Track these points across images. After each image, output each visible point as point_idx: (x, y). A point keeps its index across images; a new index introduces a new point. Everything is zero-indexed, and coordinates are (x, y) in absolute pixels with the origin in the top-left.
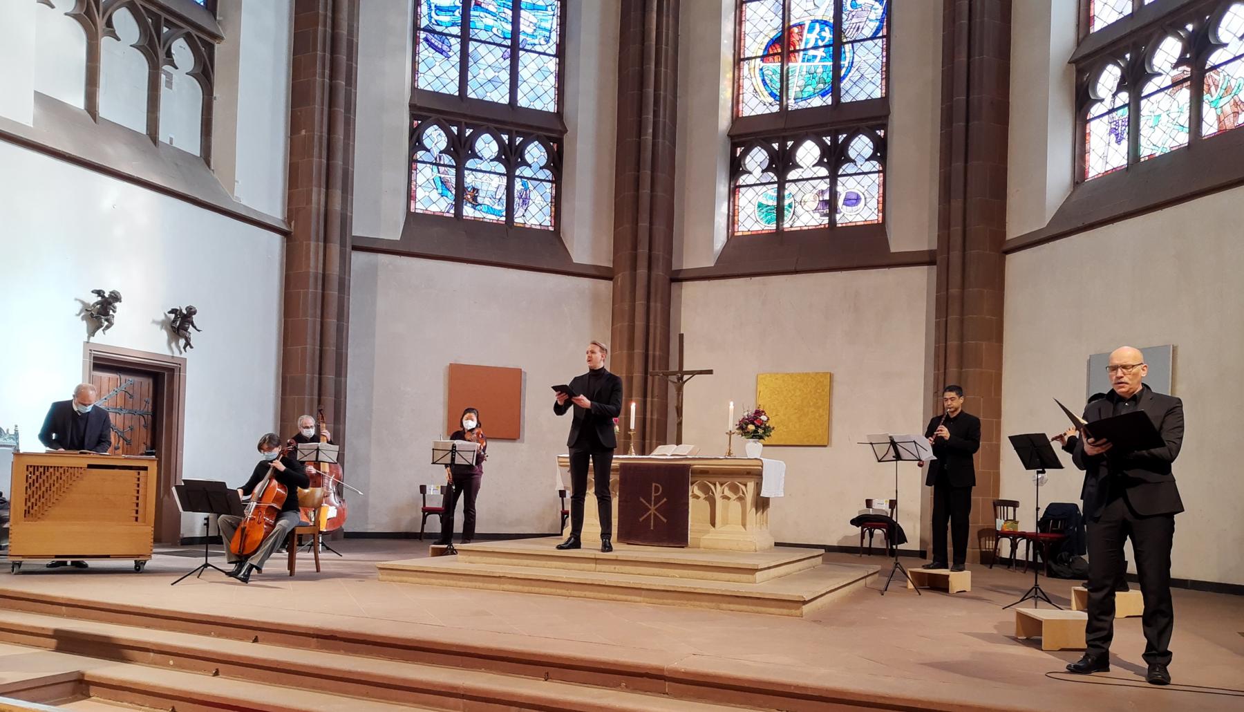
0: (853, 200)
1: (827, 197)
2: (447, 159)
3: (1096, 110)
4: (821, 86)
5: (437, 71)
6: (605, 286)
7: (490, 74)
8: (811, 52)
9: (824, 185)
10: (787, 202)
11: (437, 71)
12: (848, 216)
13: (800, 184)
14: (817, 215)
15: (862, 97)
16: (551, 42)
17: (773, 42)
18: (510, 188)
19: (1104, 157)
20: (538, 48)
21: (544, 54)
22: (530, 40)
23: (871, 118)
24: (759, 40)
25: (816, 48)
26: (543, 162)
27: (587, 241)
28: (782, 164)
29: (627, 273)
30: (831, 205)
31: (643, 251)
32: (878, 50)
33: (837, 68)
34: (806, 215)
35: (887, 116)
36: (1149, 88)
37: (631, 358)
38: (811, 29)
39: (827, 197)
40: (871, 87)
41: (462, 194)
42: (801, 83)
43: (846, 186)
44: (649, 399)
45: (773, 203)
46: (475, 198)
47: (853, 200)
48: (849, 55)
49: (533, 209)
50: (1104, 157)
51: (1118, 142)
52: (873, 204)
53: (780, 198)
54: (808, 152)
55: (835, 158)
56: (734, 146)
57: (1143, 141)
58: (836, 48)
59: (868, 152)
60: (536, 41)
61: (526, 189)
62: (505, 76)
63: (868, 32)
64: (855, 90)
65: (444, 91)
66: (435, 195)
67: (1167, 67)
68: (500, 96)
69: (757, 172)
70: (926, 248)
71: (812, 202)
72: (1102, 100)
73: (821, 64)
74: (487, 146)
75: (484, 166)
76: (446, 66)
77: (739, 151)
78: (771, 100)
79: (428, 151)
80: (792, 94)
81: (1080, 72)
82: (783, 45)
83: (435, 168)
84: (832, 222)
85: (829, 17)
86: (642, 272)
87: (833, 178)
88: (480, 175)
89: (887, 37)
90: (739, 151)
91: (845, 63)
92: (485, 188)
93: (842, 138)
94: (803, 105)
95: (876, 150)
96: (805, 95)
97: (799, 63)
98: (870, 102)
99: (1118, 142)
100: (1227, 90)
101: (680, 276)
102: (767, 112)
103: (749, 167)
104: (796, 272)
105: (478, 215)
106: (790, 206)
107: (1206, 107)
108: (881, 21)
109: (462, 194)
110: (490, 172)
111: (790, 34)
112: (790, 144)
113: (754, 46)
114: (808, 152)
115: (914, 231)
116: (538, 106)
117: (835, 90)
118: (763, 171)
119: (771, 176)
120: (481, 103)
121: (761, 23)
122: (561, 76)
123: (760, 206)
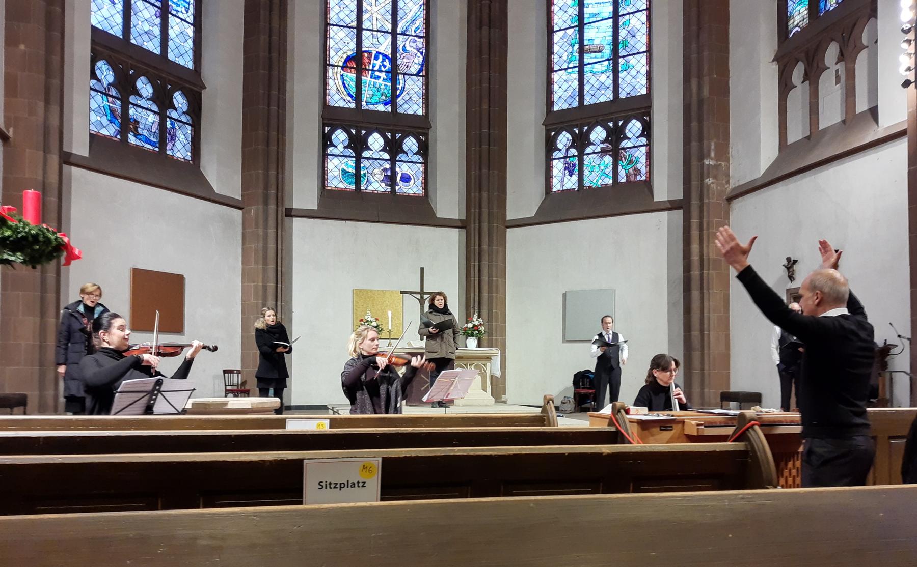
0: (406, 179)
1: (389, 173)
2: (113, 92)
3: (556, 154)
4: (384, 98)
6: (237, 214)
7: (147, 27)
8: (377, 73)
9: (388, 166)
10: (362, 172)
12: (403, 188)
13: (371, 161)
14: (383, 185)
15: (411, 112)
16: (190, 14)
17: (348, 59)
18: (162, 125)
19: (562, 181)
20: (180, 15)
24: (340, 53)
25: (380, 71)
26: (185, 109)
28: (358, 145)
29: (261, 207)
30: (391, 179)
31: (272, 192)
32: (420, 84)
33: (394, 88)
34: (376, 185)
36: (589, 150)
37: (265, 271)
38: (376, 58)
39: (389, 173)
40: (415, 107)
41: (127, 125)
43: (402, 168)
44: (279, 303)
45: (352, 171)
46: (136, 129)
47: (406, 179)
49: (178, 144)
50: (562, 181)
52: (419, 182)
53: (358, 167)
54: (376, 141)
55: (394, 148)
56: (324, 125)
57: (585, 179)
58: (394, 74)
59: (415, 148)
60: (179, 9)
61: (174, 128)
62: (157, 31)
63: (414, 69)
64: (406, 106)
65: (111, 32)
66: (105, 121)
68: (153, 47)
69: (341, 147)
70: (457, 218)
72: (560, 150)
73: (383, 83)
76: (113, 12)
77: (327, 129)
78: (349, 98)
79: (99, 81)
80: (364, 99)
81: (548, 132)
82: (357, 61)
83: (105, 97)
84: (393, 189)
85: (389, 52)
86: (272, 207)
87: (393, 161)
88: (140, 110)
89: (427, 77)
90: (327, 129)
91: (400, 87)
93: (398, 136)
94: (371, 107)
95: (420, 147)
96: (373, 102)
97: (369, 79)
98: (415, 116)
100: (631, 162)
101: (293, 213)
102: (346, 106)
103: (334, 142)
105: (139, 143)
106: (365, 174)
107: (620, 168)
108: (422, 65)
110: (147, 109)
111: (362, 56)
112: (363, 132)
113: (336, 58)
114: (376, 141)
116: (181, 62)
118: (345, 147)
119: (350, 152)
120: (139, 49)
121: (341, 44)
123: (343, 171)
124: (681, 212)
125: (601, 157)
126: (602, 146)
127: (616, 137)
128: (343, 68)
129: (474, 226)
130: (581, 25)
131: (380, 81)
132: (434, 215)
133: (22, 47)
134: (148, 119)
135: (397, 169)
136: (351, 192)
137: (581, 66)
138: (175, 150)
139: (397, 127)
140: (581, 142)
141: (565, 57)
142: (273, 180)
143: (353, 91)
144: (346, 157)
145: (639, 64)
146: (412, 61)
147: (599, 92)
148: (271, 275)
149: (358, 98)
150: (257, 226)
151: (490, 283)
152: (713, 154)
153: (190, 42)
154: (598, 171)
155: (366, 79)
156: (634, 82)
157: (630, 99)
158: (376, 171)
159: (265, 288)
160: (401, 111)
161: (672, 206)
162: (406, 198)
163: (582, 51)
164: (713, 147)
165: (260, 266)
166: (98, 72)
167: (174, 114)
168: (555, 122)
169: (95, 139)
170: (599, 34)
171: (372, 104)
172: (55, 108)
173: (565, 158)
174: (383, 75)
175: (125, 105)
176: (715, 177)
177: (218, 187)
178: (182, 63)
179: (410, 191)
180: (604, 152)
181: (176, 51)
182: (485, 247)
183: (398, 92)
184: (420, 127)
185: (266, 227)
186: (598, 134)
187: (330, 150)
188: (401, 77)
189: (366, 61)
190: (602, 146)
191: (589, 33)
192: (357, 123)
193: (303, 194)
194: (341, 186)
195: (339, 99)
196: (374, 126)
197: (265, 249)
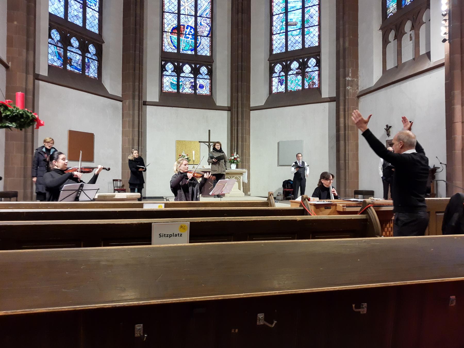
2: (60, 45)
3: (274, 75)
5: (56, 6)
6: (120, 104)
7: (76, 13)
8: (187, 36)
9: (193, 81)
10: (180, 83)
11: (56, 6)
14: (190, 90)
15: (204, 54)
16: (97, 7)
17: (174, 29)
18: (83, 61)
19: (277, 88)
20: (92, 7)
21: (94, 10)
22: (89, 3)
24: (170, 26)
25: (189, 34)
26: (94, 53)
28: (178, 70)
29: (131, 100)
30: (194, 87)
31: (137, 93)
33: (196, 43)
34: (187, 90)
35: (213, 62)
36: (290, 73)
37: (133, 131)
38: (187, 28)
40: (206, 52)
41: (66, 60)
42: (184, 45)
43: (200, 82)
44: (140, 147)
45: (175, 83)
46: (71, 62)
47: (202, 87)
48: (199, 40)
49: (91, 70)
50: (277, 88)
51: (281, 85)
52: (208, 88)
53: (178, 81)
54: (187, 68)
55: (196, 72)
56: (162, 61)
57: (288, 87)
58: (195, 36)
59: (206, 72)
60: (91, 4)
61: (89, 62)
62: (81, 15)
63: (205, 34)
64: (201, 52)
65: (58, 15)
66: (55, 59)
67: (294, 69)
68: (79, 23)
69: (170, 71)
70: (226, 106)
72: (276, 73)
73: (191, 40)
75: (73, 50)
76: (60, 6)
77: (163, 63)
78: (174, 48)
79: (53, 39)
80: (181, 48)
81: (270, 64)
82: (178, 30)
83: (55, 47)
85: (193, 25)
86: (137, 100)
87: (195, 78)
88: (72, 53)
89: (212, 37)
90: (163, 63)
91: (199, 42)
92: (74, 59)
94: (185, 52)
95: (208, 71)
97: (183, 38)
98: (206, 56)
99: (281, 85)
100: (310, 79)
102: (173, 52)
103: (167, 69)
104: (188, 108)
105: (72, 69)
106: (182, 85)
107: (305, 81)
108: (209, 32)
110: (76, 53)
111: (180, 27)
112: (181, 64)
113: (168, 28)
114: (187, 68)
116: (92, 30)
117: (195, 49)
118: (172, 72)
119: (174, 74)
121: (170, 21)
123: (171, 83)
124: (335, 103)
125: (296, 76)
126: (297, 71)
127: (303, 66)
128: (171, 33)
129: (234, 110)
130: (286, 12)
131: (189, 39)
132: (215, 104)
133: (15, 23)
134: (76, 58)
135: (197, 82)
136: (175, 93)
137: (287, 32)
138: (90, 73)
139: (197, 62)
140: (286, 69)
141: (278, 28)
142: (137, 87)
143: (176, 44)
144: (173, 76)
145: (315, 31)
146: (204, 29)
147: (295, 44)
148: (136, 133)
149: (178, 47)
150: (129, 110)
151: (242, 137)
152: (350, 75)
153: (97, 20)
154: (295, 83)
155: (182, 38)
156: (312, 40)
157: (310, 48)
158: (187, 83)
159: (133, 140)
160: (199, 54)
161: (331, 100)
162: (202, 96)
163: (287, 25)
164: (350, 71)
165: (131, 129)
166: (52, 35)
167: (89, 56)
168: (274, 59)
169: (51, 67)
170: (295, 17)
171: (185, 50)
172: (31, 53)
173: (279, 76)
174: (190, 36)
175: (65, 51)
176: (351, 86)
177: (110, 91)
178: (93, 30)
179: (203, 93)
180: (297, 74)
181: (90, 25)
182: (240, 120)
183: (198, 45)
184: (208, 62)
185: (134, 110)
186: (295, 65)
187: (165, 73)
188: (199, 37)
189: (182, 29)
190: (297, 71)
191: (290, 16)
192: (177, 60)
193: (152, 94)
194: (170, 90)
195: (169, 48)
196: (186, 61)
197: (133, 121)
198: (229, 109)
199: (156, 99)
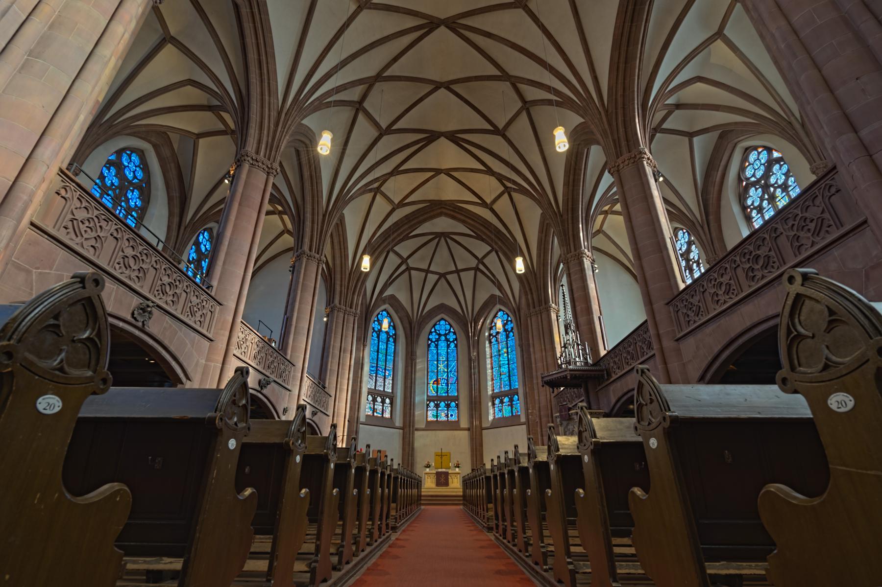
0: (452, 415)
12: (450, 418)
23: (455, 399)
27: (398, 422)
28: (437, 406)
30: (447, 416)
34: (443, 418)
41: (374, 410)
54: (442, 404)
71: (443, 415)
74: (379, 399)
109: (374, 410)
114: (442, 404)
115: (464, 424)
117: (447, 392)
122: (393, 384)
127: (511, 400)
134: (379, 407)
139: (448, 400)
149: (437, 392)
155: (440, 386)
169: (367, 416)
186: (506, 400)
198: (469, 429)
199: (423, 426)
